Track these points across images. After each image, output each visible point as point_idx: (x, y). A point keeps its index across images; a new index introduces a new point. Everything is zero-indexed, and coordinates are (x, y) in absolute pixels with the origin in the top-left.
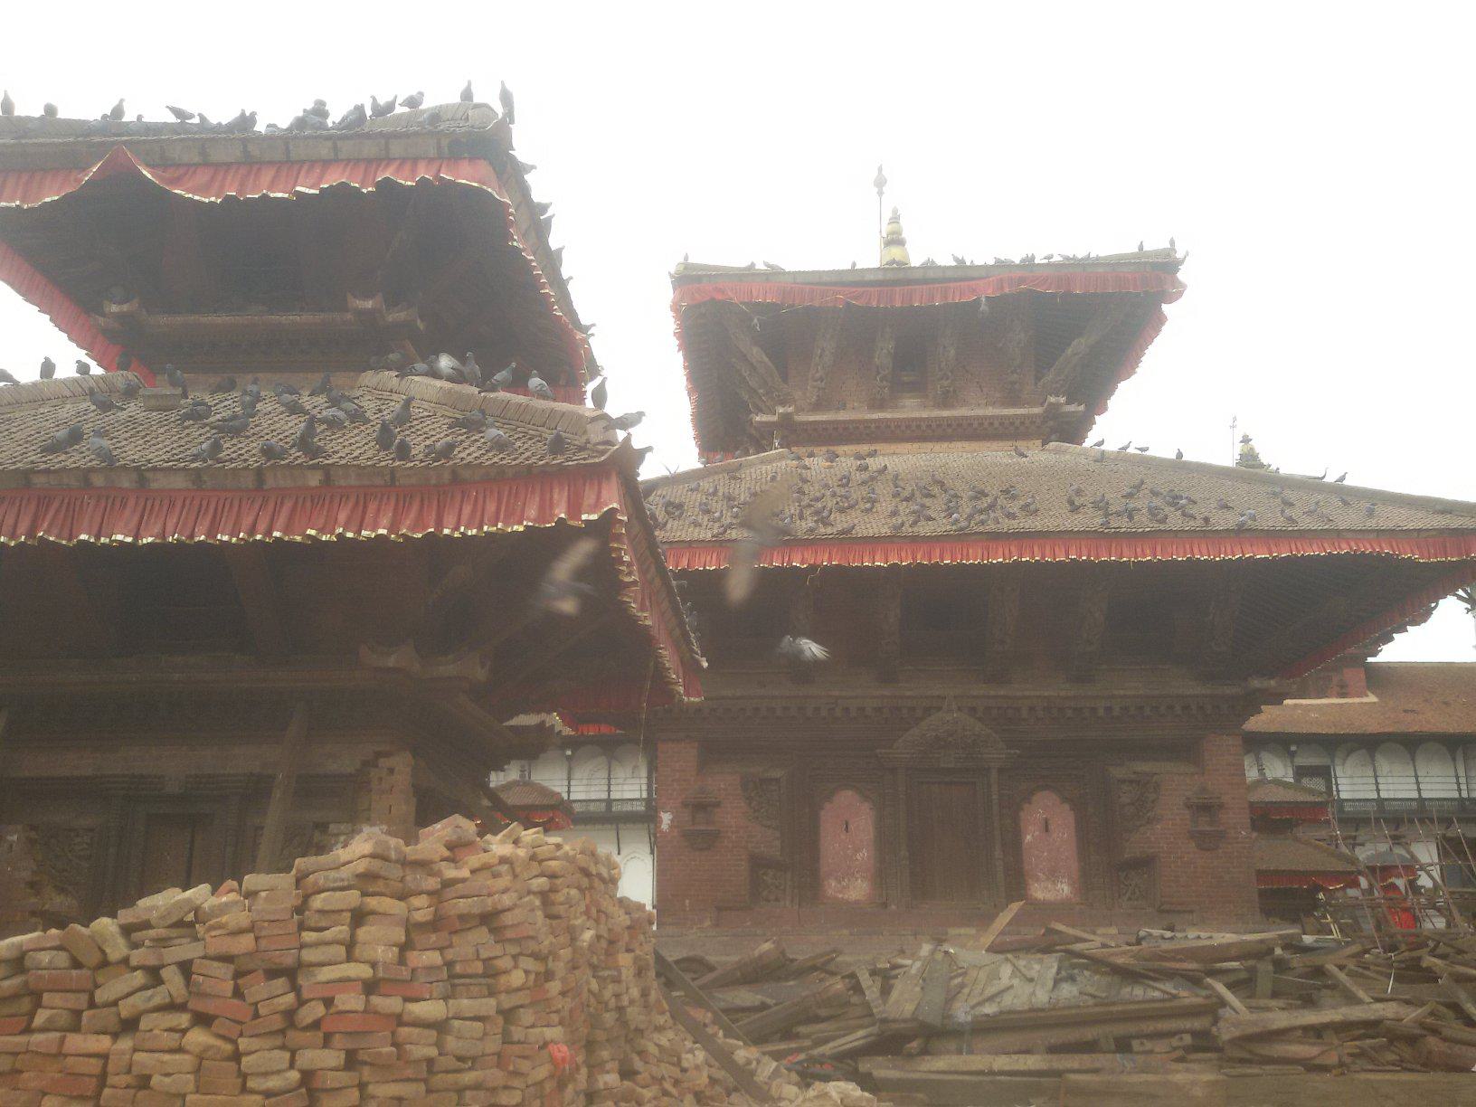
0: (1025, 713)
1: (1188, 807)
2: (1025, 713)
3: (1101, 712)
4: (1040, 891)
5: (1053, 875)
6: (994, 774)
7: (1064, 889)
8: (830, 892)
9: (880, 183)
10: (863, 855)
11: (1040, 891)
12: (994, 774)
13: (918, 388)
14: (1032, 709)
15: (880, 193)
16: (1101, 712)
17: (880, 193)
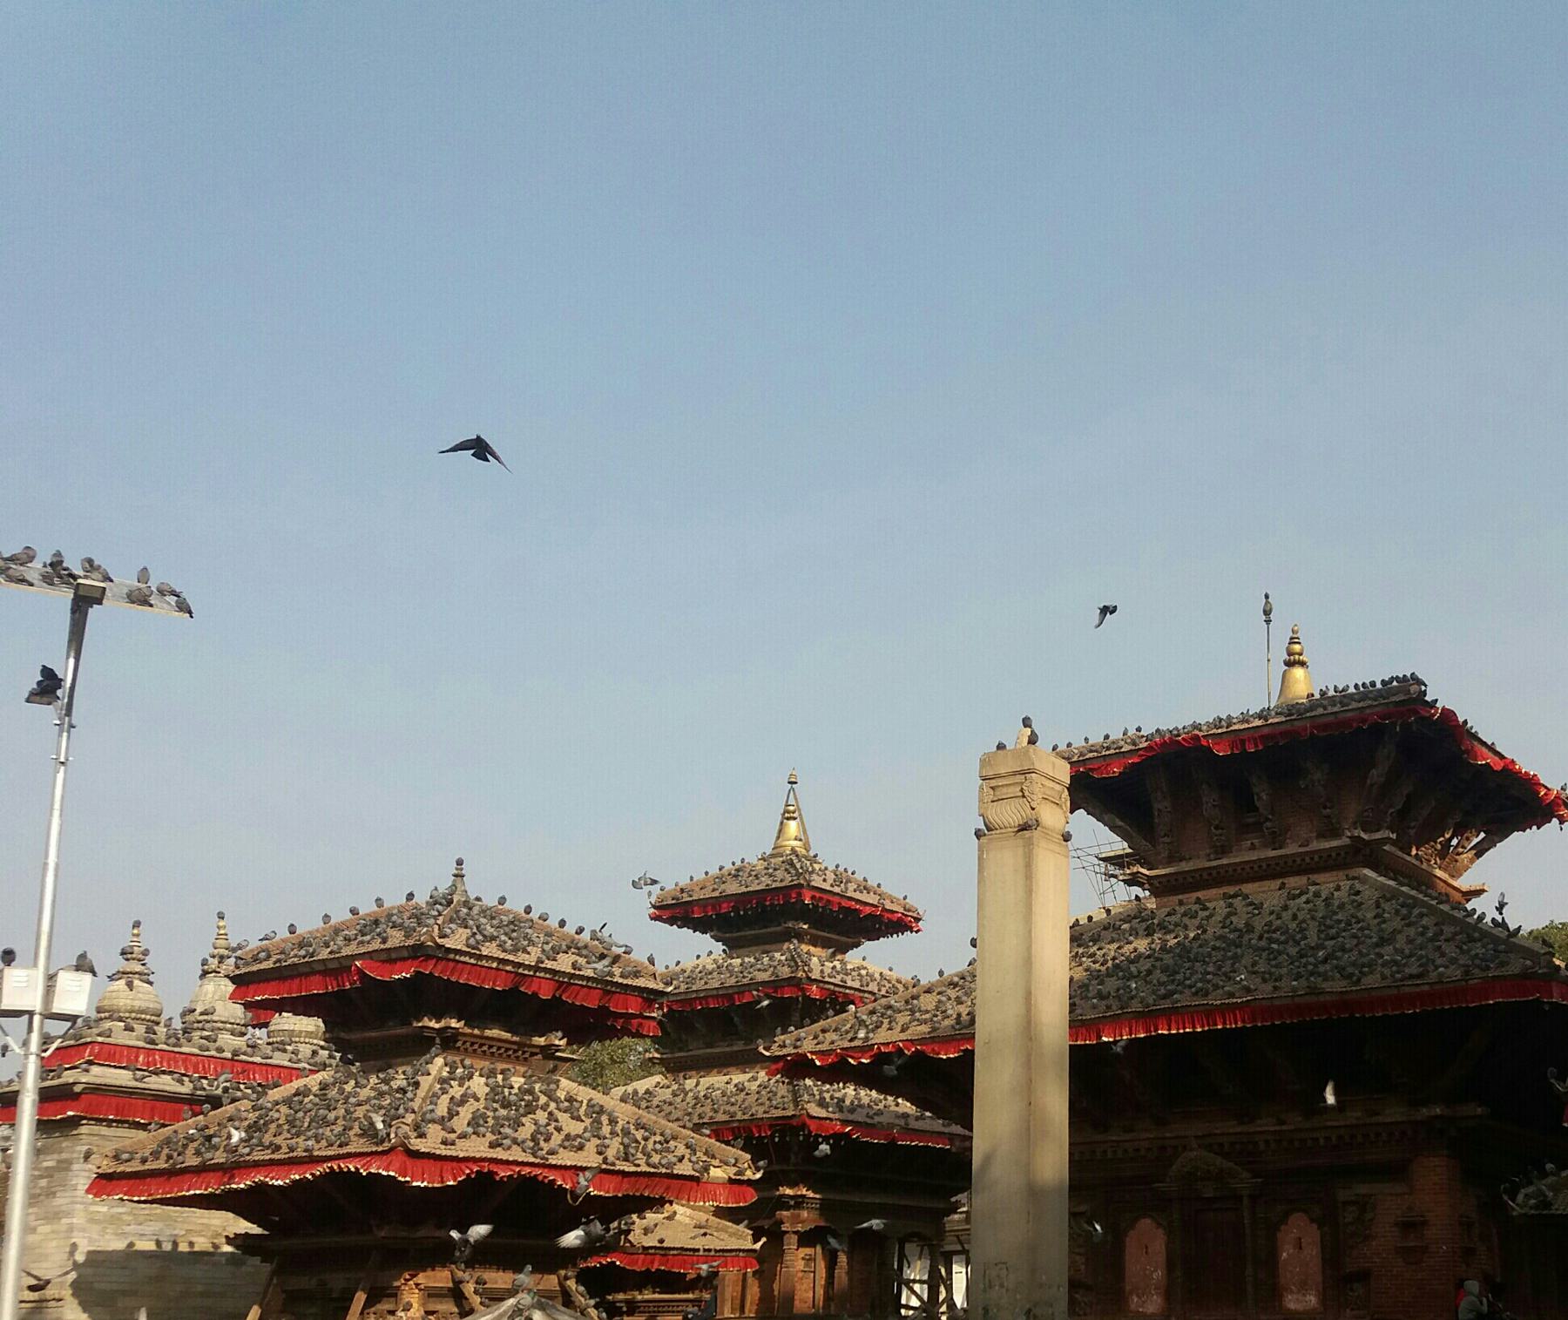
0: (1262, 1146)
1: (1396, 1224)
2: (1262, 1146)
3: (1322, 1142)
4: (1292, 1302)
5: (1303, 1287)
6: (1246, 1201)
7: (1312, 1300)
8: (1133, 1307)
9: (1267, 612)
10: (1159, 1275)
11: (1292, 1302)
12: (1246, 1201)
13: (1257, 827)
14: (1267, 1142)
15: (1268, 622)
16: (1322, 1142)
17: (1268, 622)
